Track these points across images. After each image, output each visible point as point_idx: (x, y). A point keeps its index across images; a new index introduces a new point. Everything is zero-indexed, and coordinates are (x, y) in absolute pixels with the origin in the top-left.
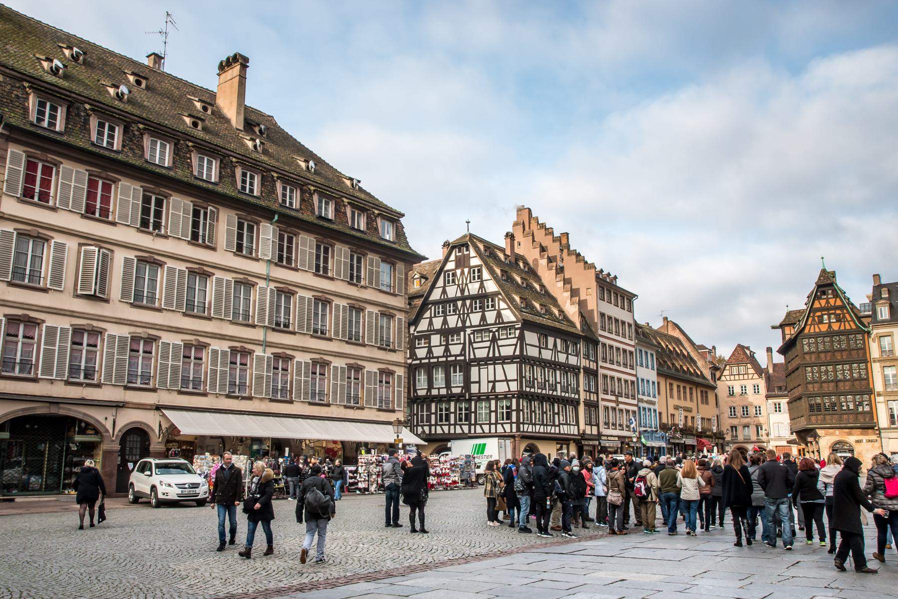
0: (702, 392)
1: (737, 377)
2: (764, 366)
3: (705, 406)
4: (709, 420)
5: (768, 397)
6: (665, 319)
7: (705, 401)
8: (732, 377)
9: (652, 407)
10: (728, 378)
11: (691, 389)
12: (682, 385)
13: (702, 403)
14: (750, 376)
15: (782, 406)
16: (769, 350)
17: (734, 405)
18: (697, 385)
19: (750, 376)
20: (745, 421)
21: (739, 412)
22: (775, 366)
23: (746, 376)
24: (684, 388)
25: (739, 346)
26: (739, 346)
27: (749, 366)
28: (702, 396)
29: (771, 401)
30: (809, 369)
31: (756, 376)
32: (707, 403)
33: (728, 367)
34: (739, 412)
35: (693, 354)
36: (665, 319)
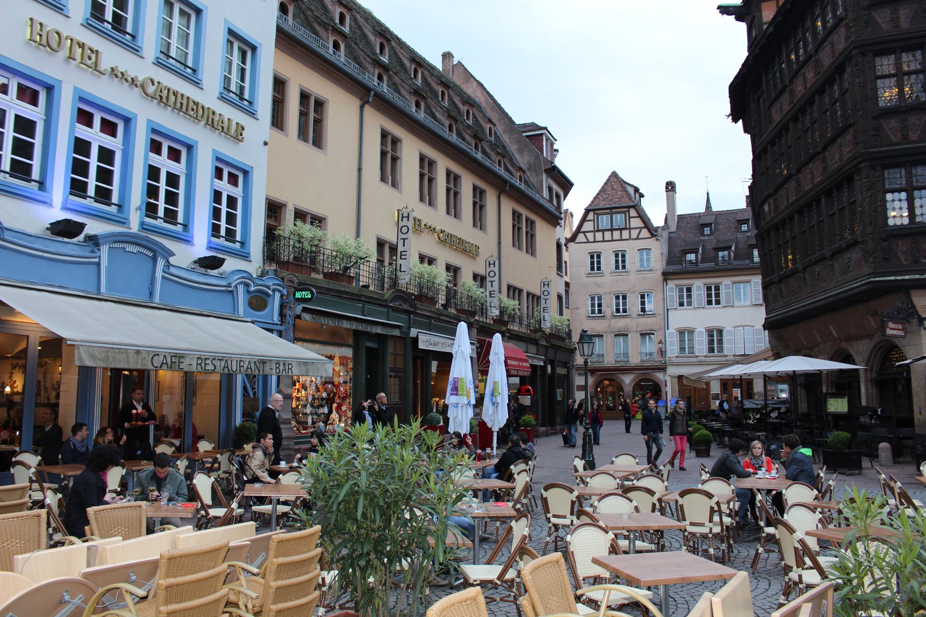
0: (516, 216)
1: (608, 235)
2: (657, 220)
3: (523, 256)
4: (535, 299)
5: (667, 276)
6: (447, 56)
7: (526, 240)
8: (599, 236)
9: (208, 146)
10: (590, 236)
11: (478, 193)
12: (443, 164)
13: (516, 243)
14: (634, 233)
15: (694, 292)
16: (670, 187)
17: (600, 291)
18: (504, 188)
19: (634, 233)
20: (620, 324)
21: (609, 306)
22: (681, 217)
23: (625, 234)
24: (453, 179)
25: (614, 175)
26: (614, 175)
27: (633, 213)
28: (516, 229)
29: (671, 284)
30: (886, 65)
31: (645, 233)
32: (531, 249)
33: (591, 216)
34: (609, 306)
35: (506, 138)
36: (447, 56)
